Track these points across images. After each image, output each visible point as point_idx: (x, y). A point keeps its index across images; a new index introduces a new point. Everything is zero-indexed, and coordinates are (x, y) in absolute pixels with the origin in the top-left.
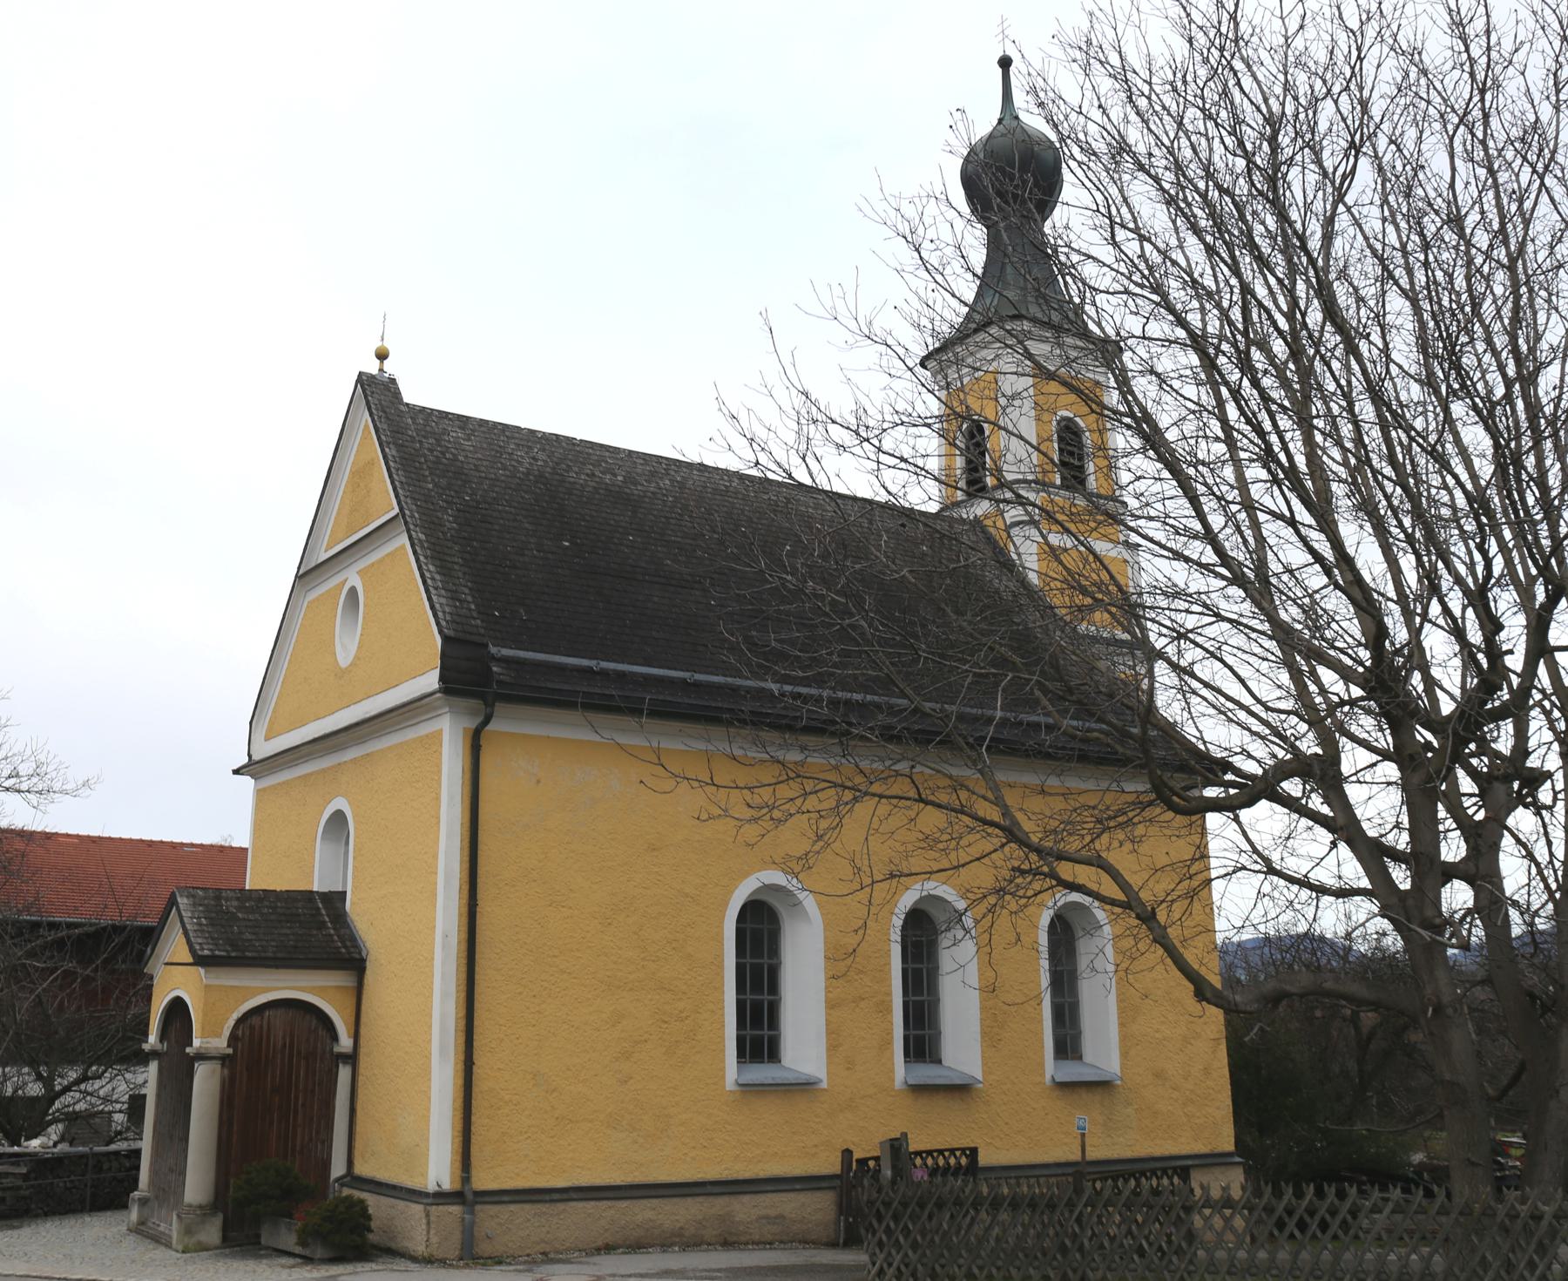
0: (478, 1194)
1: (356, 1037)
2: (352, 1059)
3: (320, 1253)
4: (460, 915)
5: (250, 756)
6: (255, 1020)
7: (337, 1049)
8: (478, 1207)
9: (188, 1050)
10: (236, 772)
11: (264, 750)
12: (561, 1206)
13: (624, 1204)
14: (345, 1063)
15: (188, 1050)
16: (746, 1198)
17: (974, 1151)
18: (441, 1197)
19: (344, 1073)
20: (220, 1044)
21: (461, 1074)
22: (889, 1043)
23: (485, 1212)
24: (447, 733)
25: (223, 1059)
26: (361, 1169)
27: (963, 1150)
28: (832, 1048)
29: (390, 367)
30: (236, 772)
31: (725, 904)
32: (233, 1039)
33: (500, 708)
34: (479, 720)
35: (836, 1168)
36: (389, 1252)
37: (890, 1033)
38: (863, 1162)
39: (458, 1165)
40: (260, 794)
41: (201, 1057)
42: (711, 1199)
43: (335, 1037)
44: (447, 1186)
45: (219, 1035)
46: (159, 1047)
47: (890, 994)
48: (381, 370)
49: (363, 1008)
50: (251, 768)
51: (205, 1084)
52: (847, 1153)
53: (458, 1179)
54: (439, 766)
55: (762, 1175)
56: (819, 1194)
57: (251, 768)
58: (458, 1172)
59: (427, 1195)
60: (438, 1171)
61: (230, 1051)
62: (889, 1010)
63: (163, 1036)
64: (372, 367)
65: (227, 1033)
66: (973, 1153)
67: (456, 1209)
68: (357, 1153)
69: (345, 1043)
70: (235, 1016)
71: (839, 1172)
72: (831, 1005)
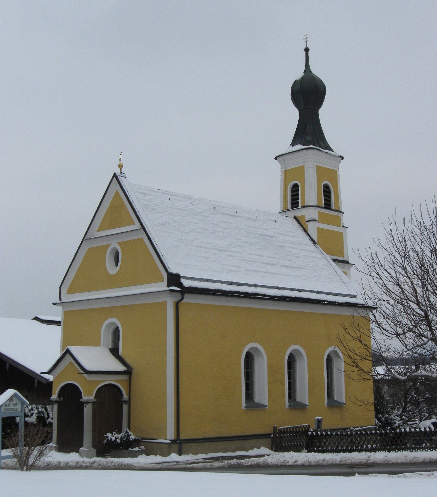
1: (129, 395)
2: (128, 402)
7: (122, 399)
9: (81, 400)
12: (202, 444)
13: (218, 443)
14: (125, 403)
15: (81, 400)
16: (249, 441)
19: (125, 407)
22: (284, 395)
25: (94, 403)
28: (269, 396)
34: (180, 298)
37: (284, 391)
41: (88, 402)
45: (92, 396)
46: (58, 399)
47: (284, 380)
49: (132, 386)
51: (88, 411)
52: (275, 428)
55: (252, 434)
60: (171, 434)
61: (96, 400)
62: (284, 385)
69: (125, 397)
72: (269, 383)
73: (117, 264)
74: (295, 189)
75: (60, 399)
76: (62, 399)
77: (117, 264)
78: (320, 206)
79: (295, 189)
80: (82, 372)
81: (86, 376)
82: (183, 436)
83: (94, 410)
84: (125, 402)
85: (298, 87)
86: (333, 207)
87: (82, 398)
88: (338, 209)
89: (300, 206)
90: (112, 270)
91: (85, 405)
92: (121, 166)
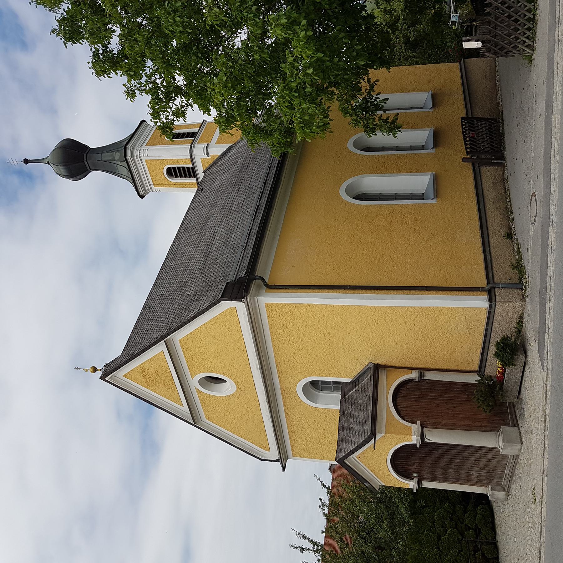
0: (488, 283)
2: (422, 371)
3: (521, 358)
4: (354, 293)
5: (277, 461)
6: (403, 413)
7: (417, 380)
8: (496, 281)
9: (418, 446)
10: (284, 469)
11: (274, 454)
14: (424, 376)
15: (418, 446)
17: (462, 118)
18: (491, 299)
19: (429, 376)
20: (415, 428)
21: (431, 292)
23: (498, 276)
24: (267, 300)
25: (423, 426)
26: (476, 367)
27: (462, 122)
29: (100, 366)
30: (284, 469)
31: (354, 205)
32: (412, 422)
33: (258, 273)
35: (469, 165)
36: (519, 329)
38: (468, 153)
39: (475, 293)
40: (296, 455)
41: (422, 436)
42: (486, 205)
43: (411, 380)
44: (486, 297)
46: (415, 480)
48: (101, 370)
50: (282, 460)
51: (435, 437)
53: (482, 293)
54: (283, 305)
55: (474, 191)
56: (482, 172)
57: (282, 460)
58: (479, 293)
59: (491, 306)
61: (419, 422)
63: (410, 478)
64: (99, 374)
65: (410, 424)
66: (462, 118)
67: (497, 291)
68: (468, 369)
69: (414, 375)
70: (401, 420)
71: (471, 164)
73: (224, 381)
74: (172, 172)
75: (415, 477)
76: (414, 475)
77: (224, 381)
78: (191, 142)
79: (172, 172)
80: (372, 442)
81: (378, 436)
82: (483, 283)
83: (435, 426)
84: (421, 375)
85: (62, 170)
86: (196, 130)
87: (415, 445)
88: (199, 126)
89: (191, 166)
90: (228, 389)
91: (426, 440)
92: (95, 370)
